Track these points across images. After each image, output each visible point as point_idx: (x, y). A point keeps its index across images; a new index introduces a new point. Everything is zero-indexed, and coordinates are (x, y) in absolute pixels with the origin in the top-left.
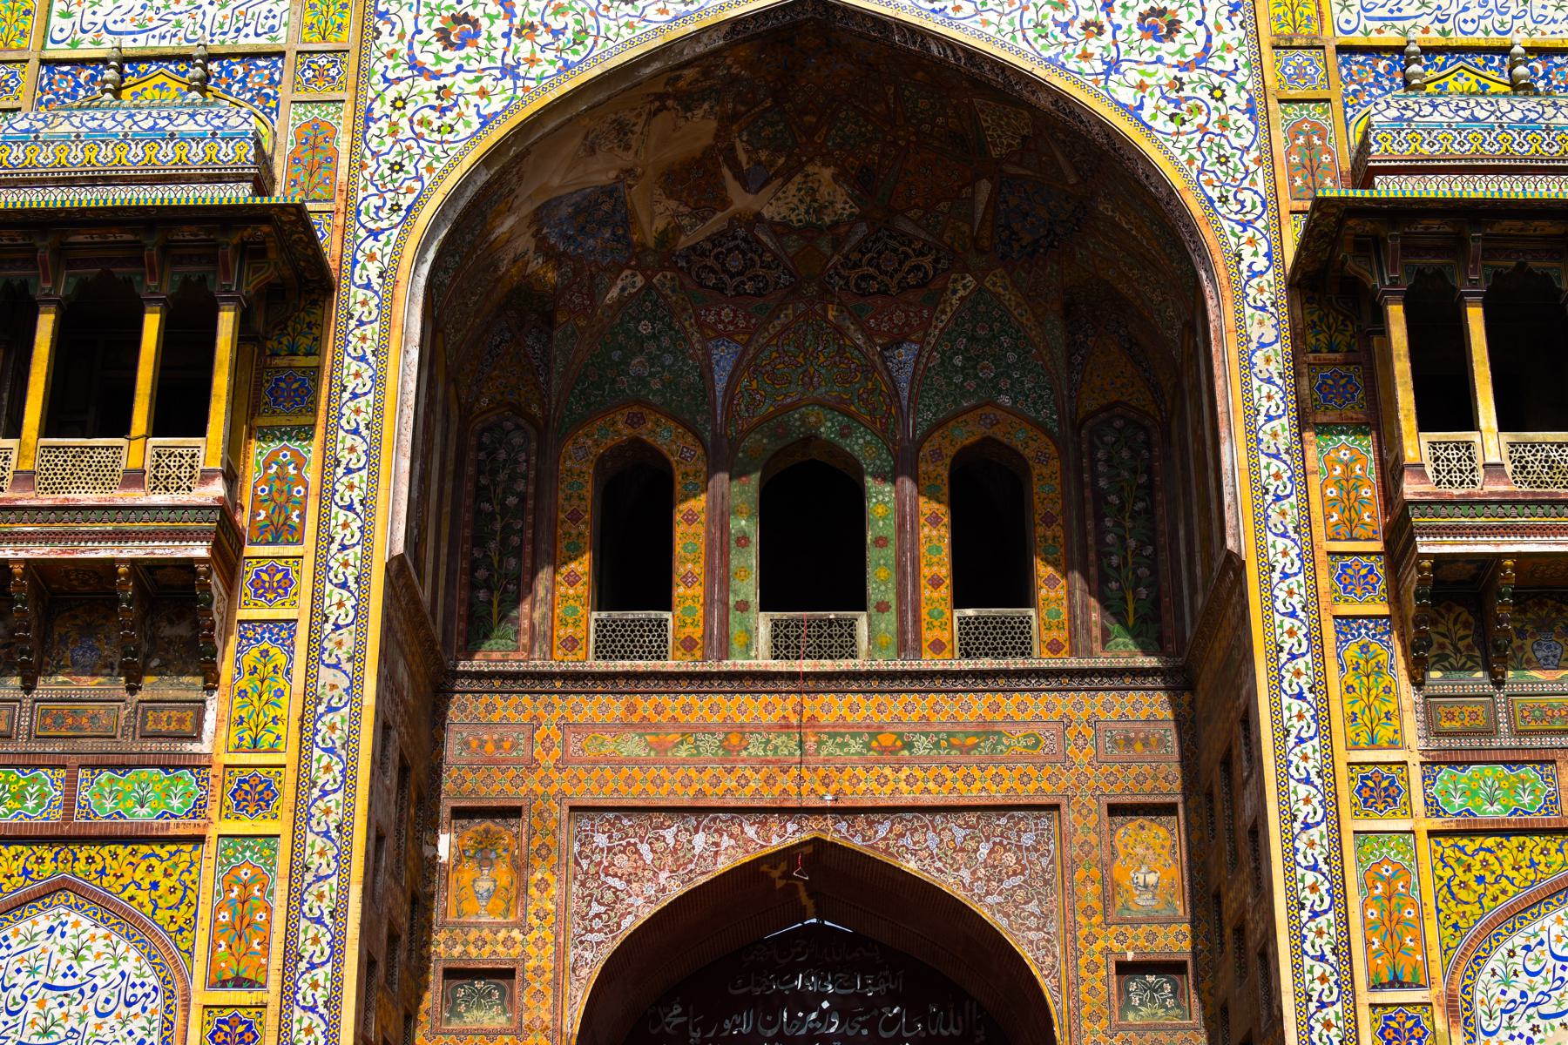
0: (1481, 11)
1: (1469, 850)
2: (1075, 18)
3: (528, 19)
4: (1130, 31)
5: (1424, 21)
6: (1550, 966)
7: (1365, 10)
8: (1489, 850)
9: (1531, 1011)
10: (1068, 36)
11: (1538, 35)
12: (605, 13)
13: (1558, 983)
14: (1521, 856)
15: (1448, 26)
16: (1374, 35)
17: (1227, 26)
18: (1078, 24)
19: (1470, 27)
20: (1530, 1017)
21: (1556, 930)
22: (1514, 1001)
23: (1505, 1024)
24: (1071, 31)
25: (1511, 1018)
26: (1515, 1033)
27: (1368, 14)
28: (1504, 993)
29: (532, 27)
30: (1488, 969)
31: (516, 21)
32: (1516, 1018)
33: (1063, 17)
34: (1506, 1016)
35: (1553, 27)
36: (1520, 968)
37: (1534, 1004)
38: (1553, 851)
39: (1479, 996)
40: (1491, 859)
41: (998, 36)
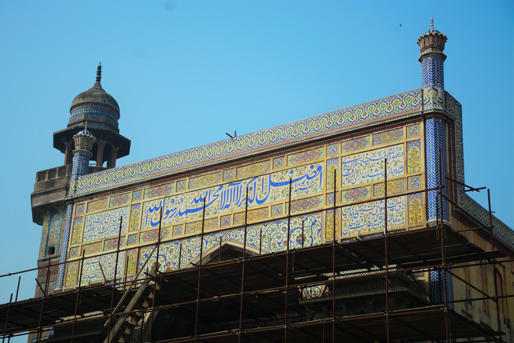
0: (380, 221)
2: (282, 241)
3: (169, 261)
4: (294, 243)
5: (364, 227)
7: (350, 226)
10: (280, 246)
11: (394, 226)
12: (184, 256)
15: (371, 227)
16: (352, 233)
17: (317, 236)
18: (283, 242)
19: (375, 227)
24: (281, 245)
27: (351, 227)
29: (170, 263)
31: (167, 262)
33: (279, 241)
35: (399, 222)
41: (265, 249)
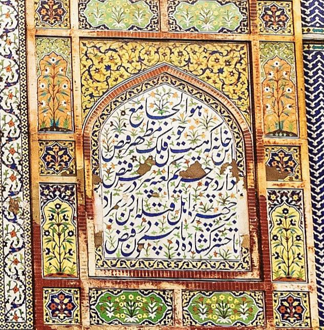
1: (103, 50)
6: (145, 122)
8: (115, 50)
9: (133, 148)
13: (149, 132)
14: (133, 55)
20: (132, 151)
21: (151, 100)
22: (122, 141)
23: (116, 155)
25: (120, 151)
26: (122, 160)
28: (117, 136)
30: (109, 122)
32: (123, 151)
34: (117, 151)
36: (127, 122)
37: (135, 144)
38: (153, 53)
39: (102, 138)
40: (115, 55)
